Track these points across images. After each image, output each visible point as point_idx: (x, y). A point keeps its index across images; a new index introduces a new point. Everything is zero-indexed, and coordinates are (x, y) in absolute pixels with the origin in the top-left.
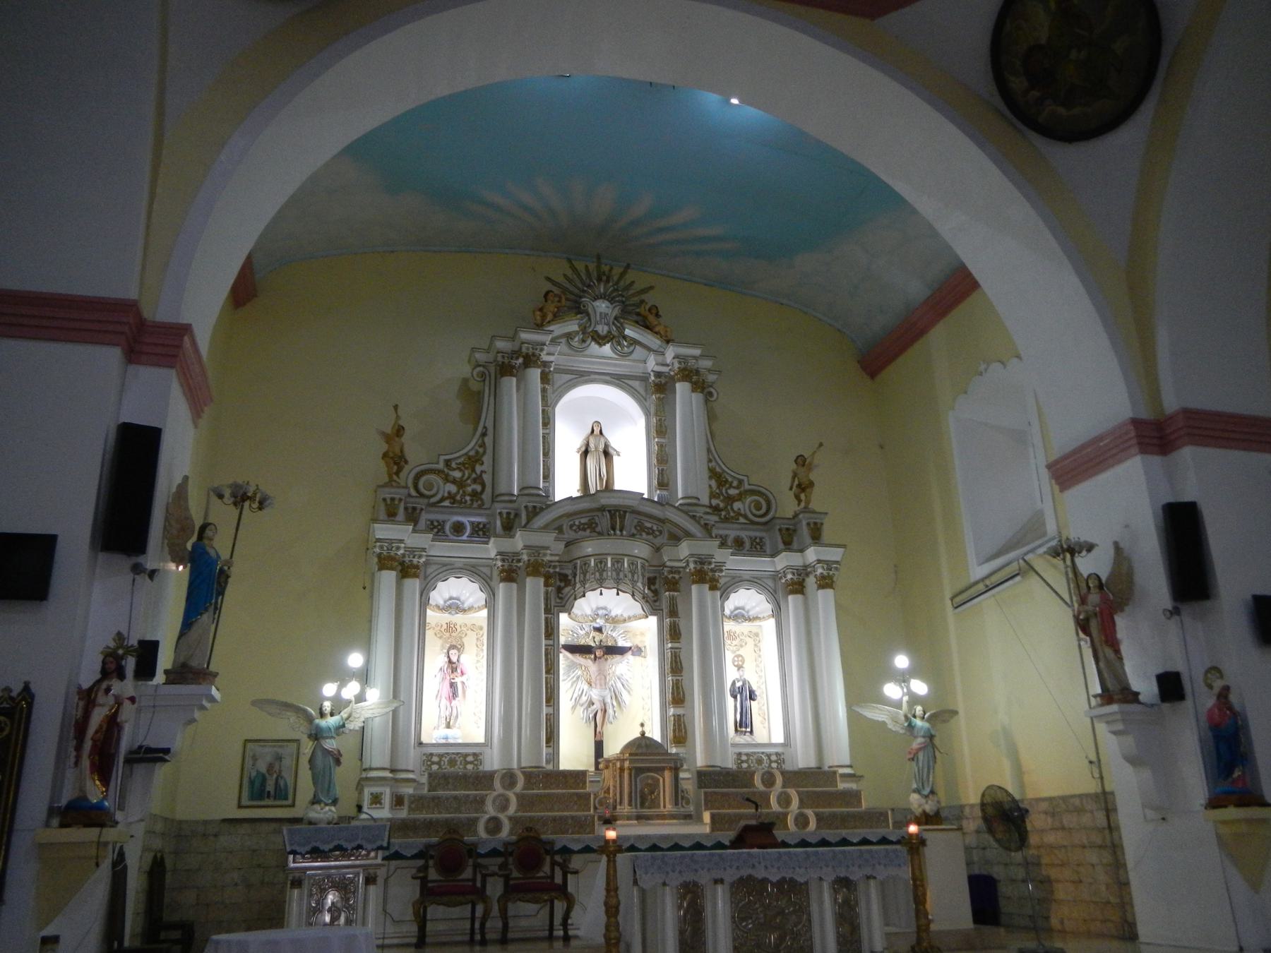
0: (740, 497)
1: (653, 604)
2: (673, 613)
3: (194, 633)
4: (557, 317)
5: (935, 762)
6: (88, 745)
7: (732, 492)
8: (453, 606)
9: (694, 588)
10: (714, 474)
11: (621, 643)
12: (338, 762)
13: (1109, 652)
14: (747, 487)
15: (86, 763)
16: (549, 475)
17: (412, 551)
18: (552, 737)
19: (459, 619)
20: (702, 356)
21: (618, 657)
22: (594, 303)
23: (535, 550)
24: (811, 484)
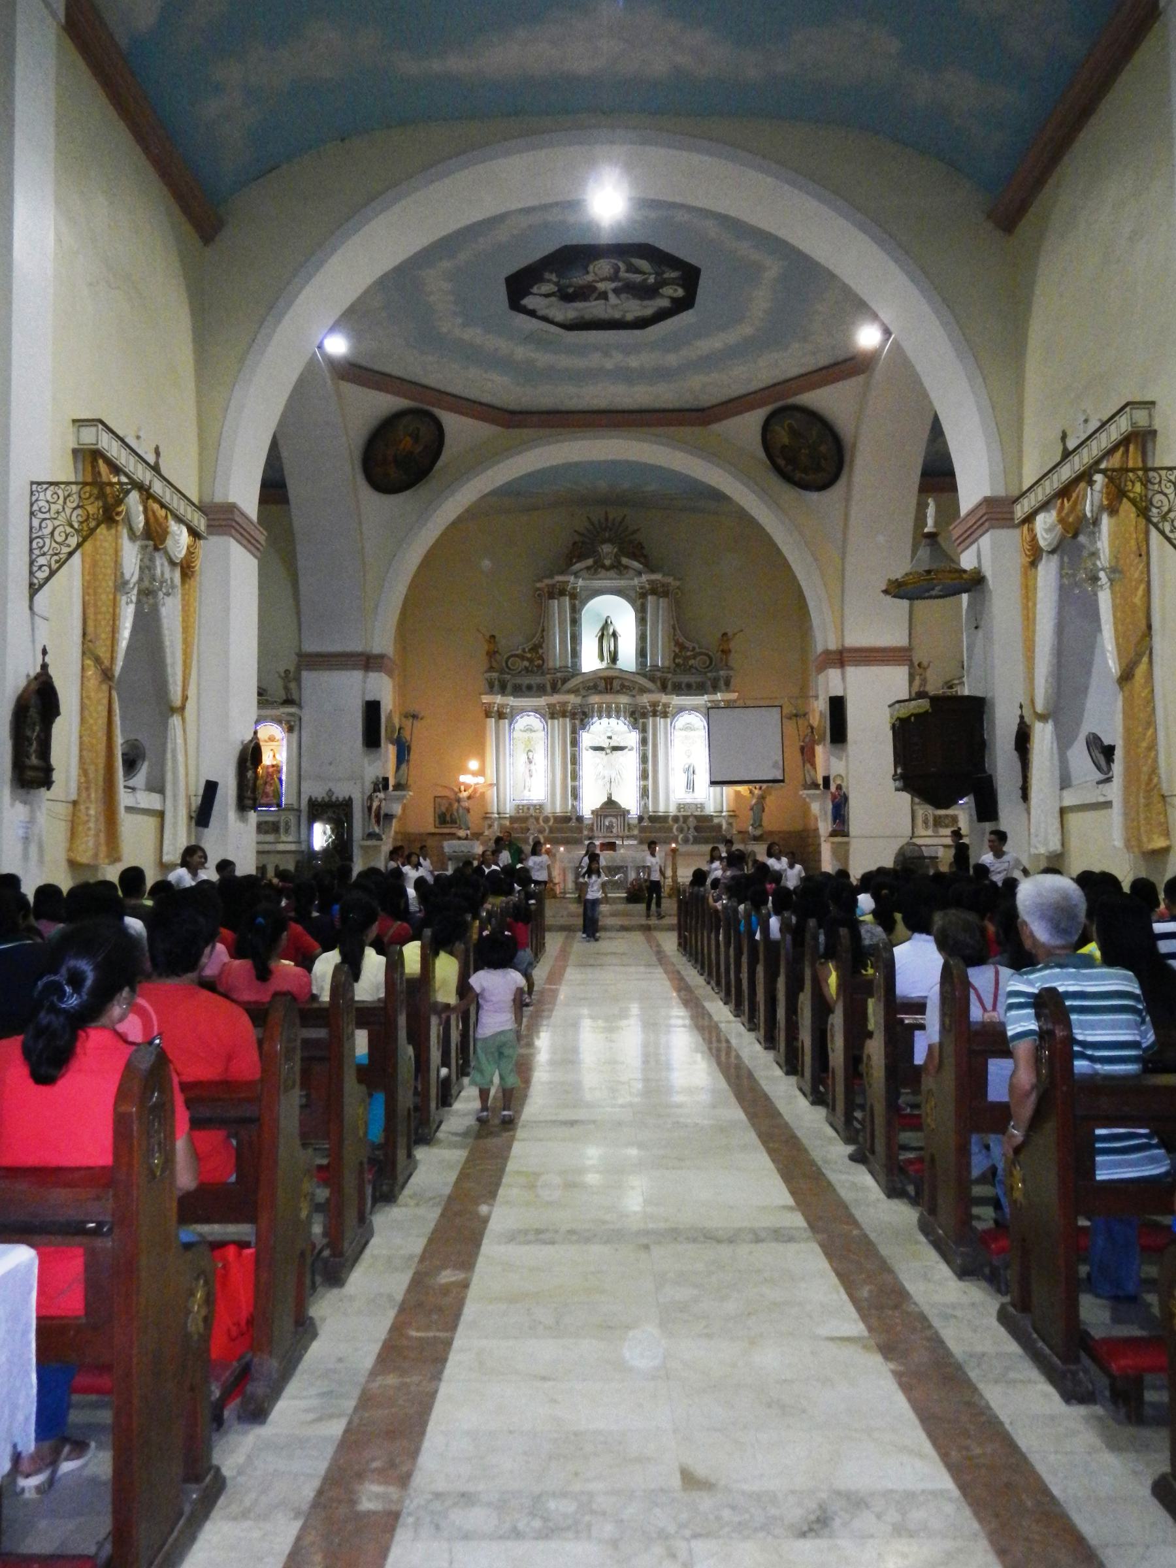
0: (694, 657)
1: (634, 725)
2: (644, 730)
3: (401, 772)
4: (581, 558)
5: (763, 811)
6: (373, 814)
7: (689, 654)
8: (529, 729)
9: (651, 719)
10: (677, 643)
11: (622, 744)
12: (468, 810)
13: (808, 766)
14: (698, 650)
15: (373, 820)
16: (576, 654)
17: (503, 706)
18: (575, 795)
19: (533, 734)
20: (664, 576)
21: (620, 752)
22: (603, 546)
23: (565, 704)
24: (730, 651)
